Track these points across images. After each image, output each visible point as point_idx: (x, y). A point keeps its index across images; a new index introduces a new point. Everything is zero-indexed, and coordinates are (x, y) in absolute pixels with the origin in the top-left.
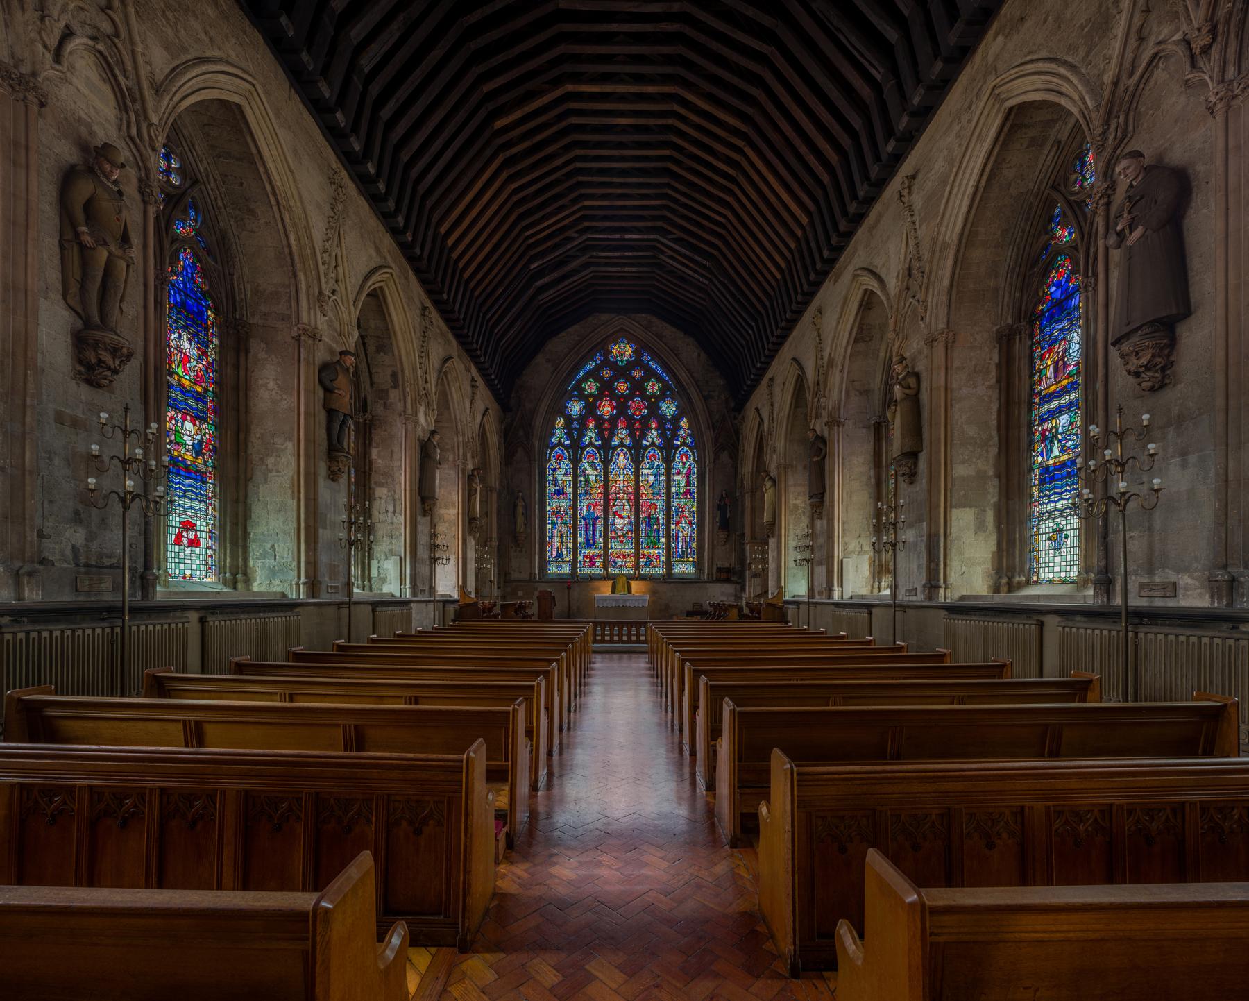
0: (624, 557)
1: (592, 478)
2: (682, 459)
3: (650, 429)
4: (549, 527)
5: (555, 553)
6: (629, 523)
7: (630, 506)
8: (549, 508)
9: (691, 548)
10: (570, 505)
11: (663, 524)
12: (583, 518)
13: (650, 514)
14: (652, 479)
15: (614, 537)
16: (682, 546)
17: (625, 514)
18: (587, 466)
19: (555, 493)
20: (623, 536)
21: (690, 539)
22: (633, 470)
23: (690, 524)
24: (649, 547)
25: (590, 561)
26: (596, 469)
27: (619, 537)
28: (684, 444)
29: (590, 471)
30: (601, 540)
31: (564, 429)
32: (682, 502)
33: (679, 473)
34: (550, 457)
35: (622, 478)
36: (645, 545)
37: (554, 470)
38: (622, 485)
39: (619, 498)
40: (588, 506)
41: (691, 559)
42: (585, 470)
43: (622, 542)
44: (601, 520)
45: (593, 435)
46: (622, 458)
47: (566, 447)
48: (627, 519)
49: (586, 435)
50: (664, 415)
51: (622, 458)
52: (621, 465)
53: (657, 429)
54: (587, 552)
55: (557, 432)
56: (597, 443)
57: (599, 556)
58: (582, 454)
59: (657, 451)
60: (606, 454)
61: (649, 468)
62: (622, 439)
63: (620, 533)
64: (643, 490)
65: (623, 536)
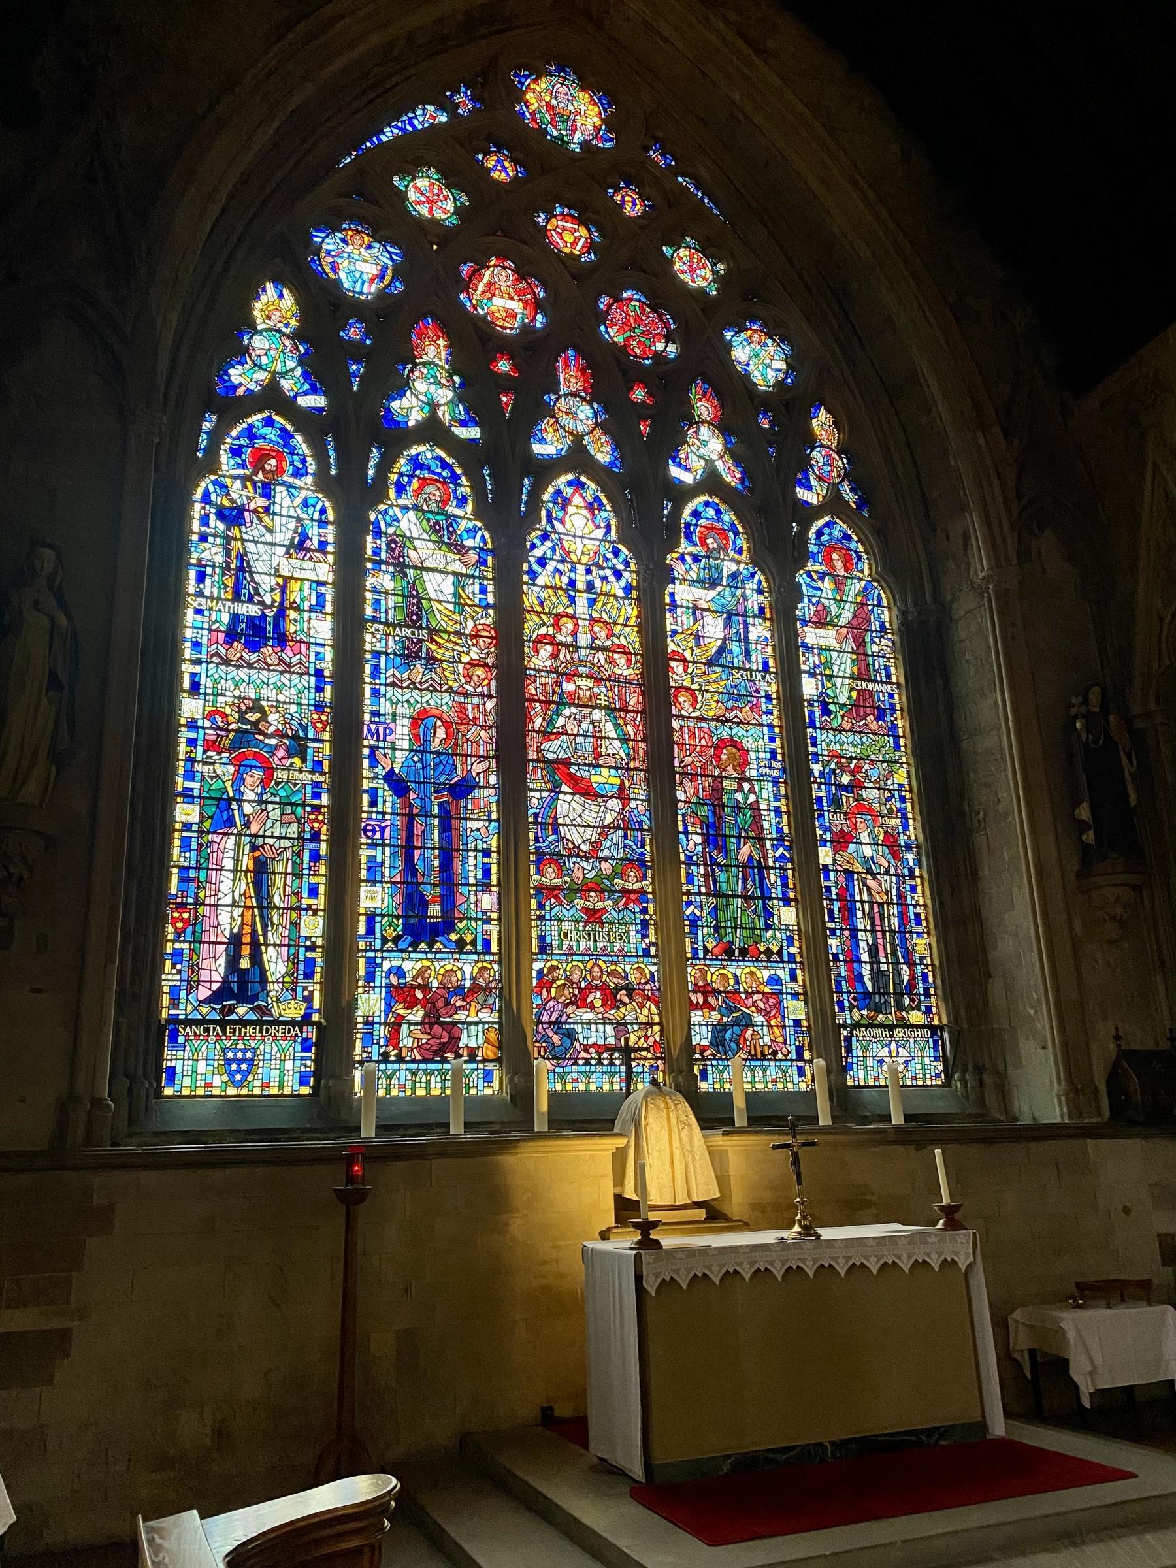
0: (611, 999)
1: (439, 588)
2: (829, 560)
3: (692, 421)
4: (186, 813)
5: (214, 970)
6: (625, 824)
7: (624, 739)
8: (190, 708)
9: (911, 964)
10: (319, 707)
11: (780, 840)
12: (390, 777)
13: (717, 791)
14: (714, 629)
15: (552, 891)
16: (873, 950)
17: (604, 779)
18: (409, 524)
19: (231, 636)
20: (601, 887)
21: (903, 916)
22: (629, 577)
23: (892, 844)
24: (729, 952)
25: (431, 1021)
26: (458, 548)
27: (583, 889)
28: (833, 504)
29: (425, 551)
30: (488, 901)
31: (297, 336)
32: (849, 746)
33: (823, 621)
34: (213, 451)
35: (582, 606)
36: (706, 938)
37: (233, 516)
38: (583, 639)
39: (572, 700)
40: (415, 722)
41: (916, 1017)
42: (399, 545)
43: (594, 916)
44: (487, 797)
45: (445, 395)
46: (577, 519)
47: (306, 421)
48: (615, 804)
49: (402, 387)
50: (745, 379)
51: (577, 519)
52: (577, 548)
53: (723, 427)
54: (410, 966)
55: (259, 343)
56: (463, 433)
57: (475, 991)
58: (385, 466)
59: (728, 517)
60: (506, 491)
61: (700, 582)
62: (578, 439)
63: (583, 870)
64: (678, 674)
65: (601, 887)
